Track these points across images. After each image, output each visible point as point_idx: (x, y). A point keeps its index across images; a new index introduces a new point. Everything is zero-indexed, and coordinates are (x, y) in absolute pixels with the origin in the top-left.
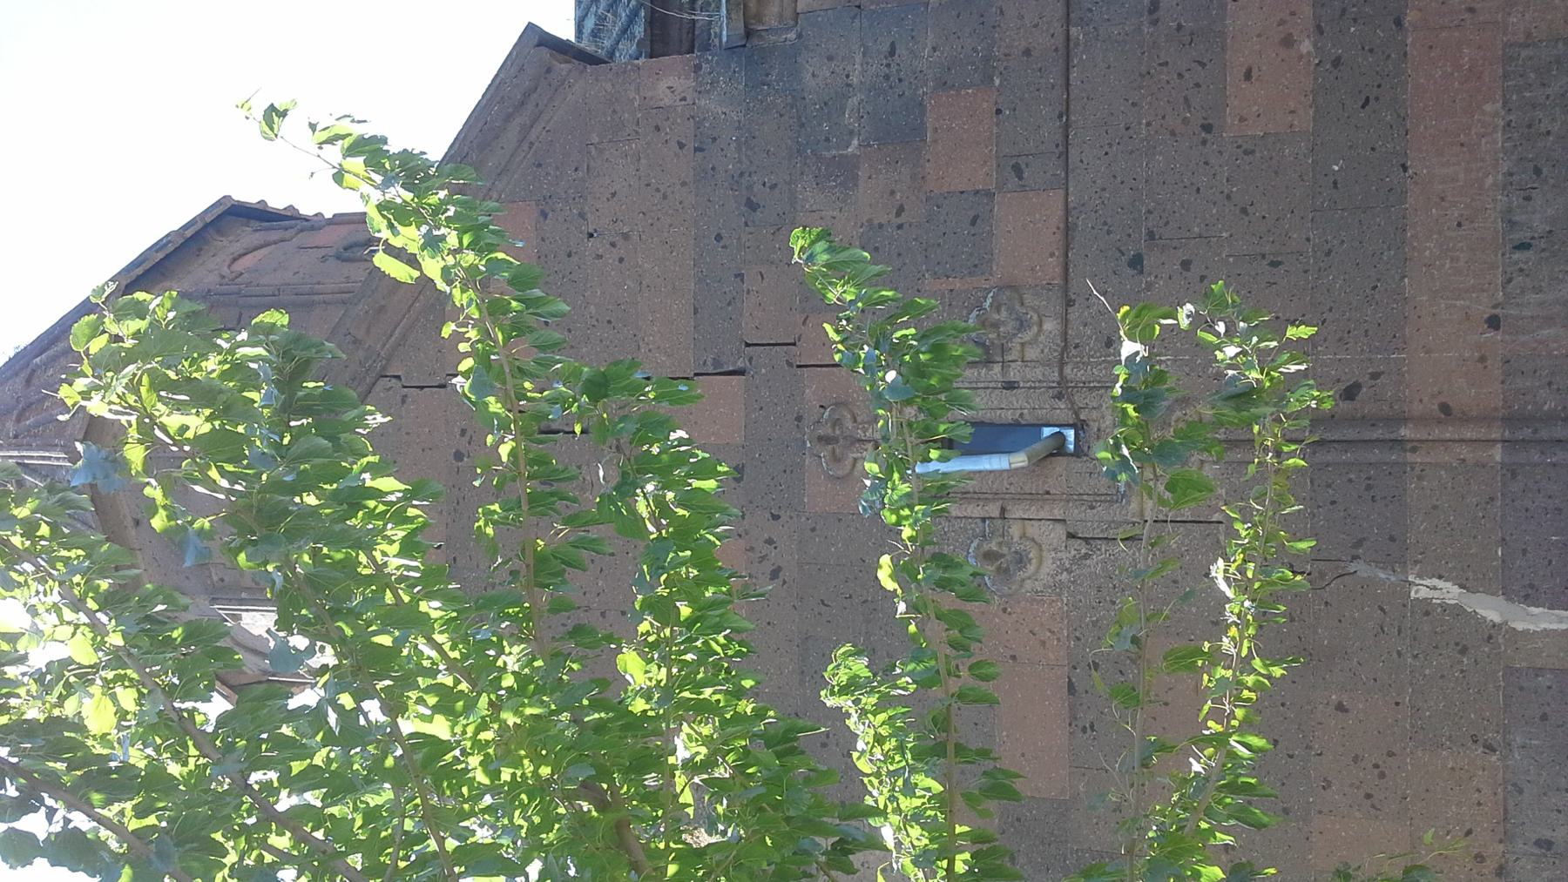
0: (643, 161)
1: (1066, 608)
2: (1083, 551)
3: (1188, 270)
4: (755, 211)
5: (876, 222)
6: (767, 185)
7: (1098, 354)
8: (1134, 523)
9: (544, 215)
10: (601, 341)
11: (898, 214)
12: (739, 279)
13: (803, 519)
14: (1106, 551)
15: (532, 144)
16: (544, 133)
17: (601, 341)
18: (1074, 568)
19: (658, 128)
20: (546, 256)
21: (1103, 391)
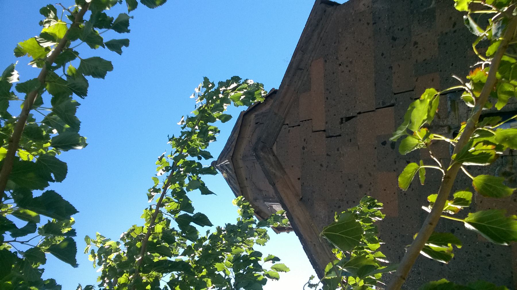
0: (356, 33)
10: (344, 102)
11: (454, 26)
12: (390, 69)
15: (321, 39)
17: (344, 102)
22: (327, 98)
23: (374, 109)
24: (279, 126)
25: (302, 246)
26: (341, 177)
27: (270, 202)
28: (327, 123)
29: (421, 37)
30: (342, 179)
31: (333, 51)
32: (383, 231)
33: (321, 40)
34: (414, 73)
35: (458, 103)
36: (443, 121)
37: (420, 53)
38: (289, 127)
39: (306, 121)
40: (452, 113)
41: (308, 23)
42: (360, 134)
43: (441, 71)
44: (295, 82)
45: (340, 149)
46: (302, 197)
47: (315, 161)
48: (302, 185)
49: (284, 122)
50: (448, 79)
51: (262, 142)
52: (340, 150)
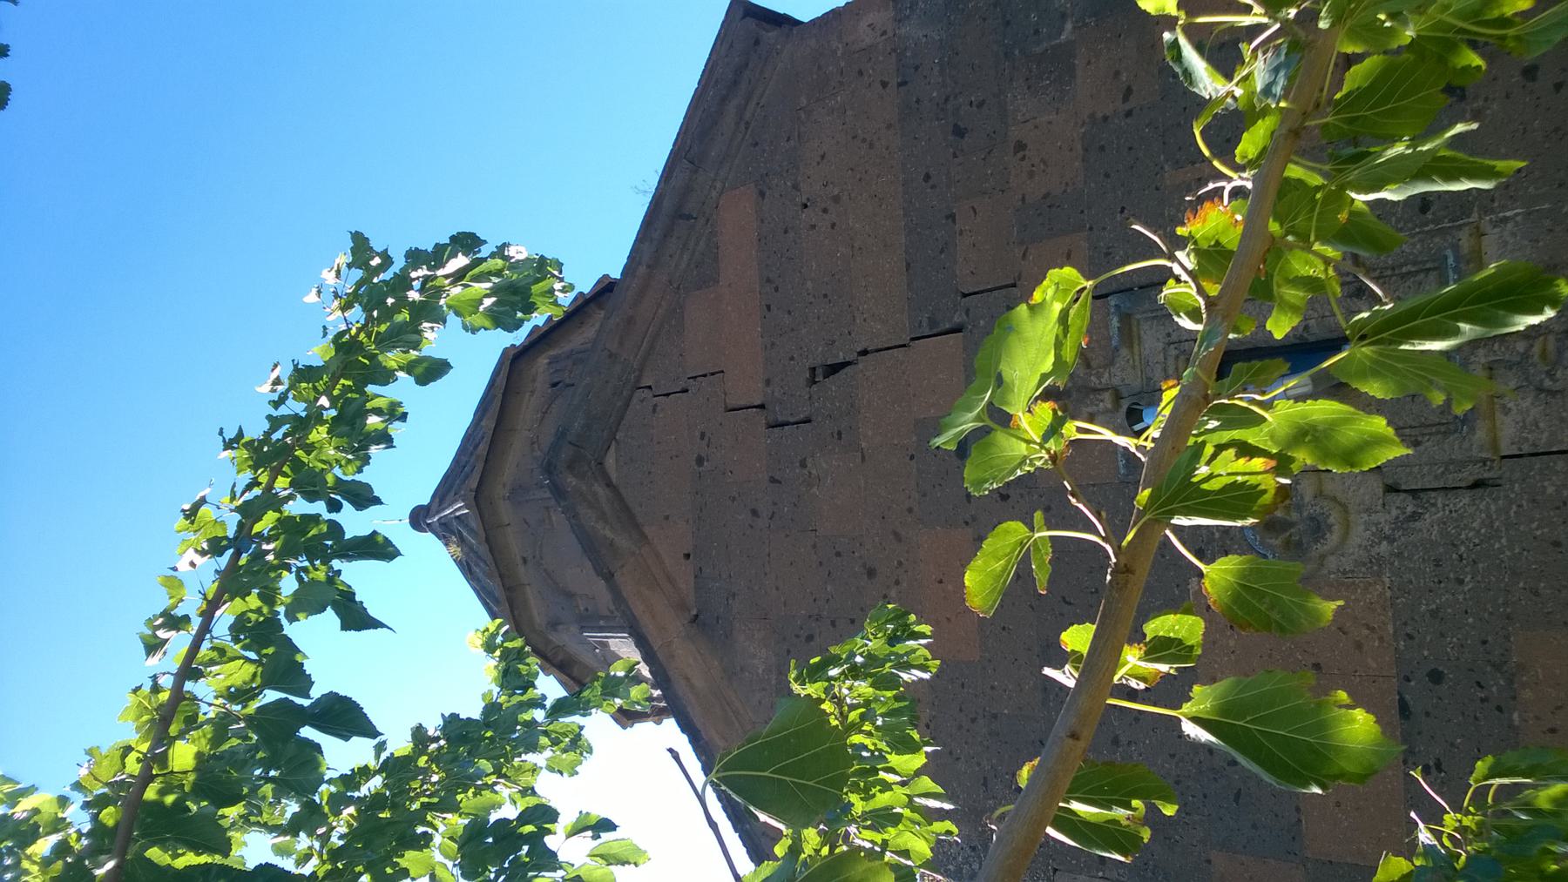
0: (848, 113)
1: (1389, 594)
2: (1410, 509)
3: (1534, 79)
4: (962, 137)
5: (1099, 115)
6: (974, 104)
7: (1410, 225)
8: (1484, 462)
9: (762, 194)
10: (819, 318)
11: (1126, 99)
12: (950, 220)
13: (1036, 496)
14: (1444, 505)
15: (747, 123)
16: (759, 110)
17: (819, 318)
18: (1398, 534)
19: (861, 73)
20: (766, 238)
21: (1422, 276)
22: (769, 307)
23: (905, 339)
24: (625, 393)
25: (700, 765)
26: (814, 546)
27: (601, 629)
28: (768, 382)
29: (1036, 127)
30: (815, 553)
31: (785, 163)
32: (936, 704)
33: (747, 128)
34: (1016, 232)
35: (1138, 324)
36: (1099, 376)
37: (1031, 175)
38: (655, 396)
39: (705, 376)
40: (1124, 352)
41: (705, 77)
42: (867, 415)
43: (1091, 229)
44: (671, 256)
45: (809, 462)
46: (699, 611)
47: (734, 499)
48: (696, 577)
49: (638, 379)
50: (1110, 254)
51: (570, 443)
52: (809, 465)
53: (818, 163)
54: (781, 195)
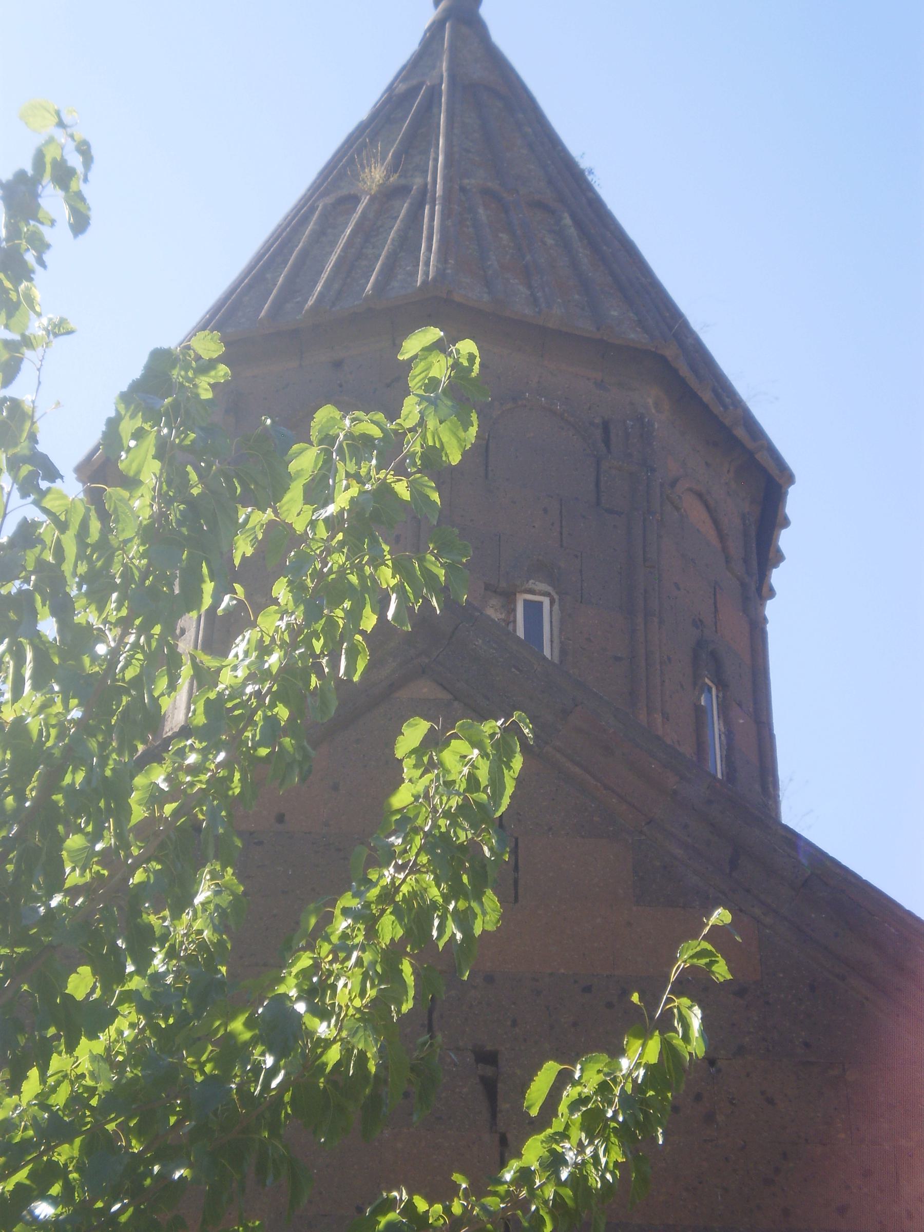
22: (587, 989)
53: (763, 1093)
54: (733, 1025)
